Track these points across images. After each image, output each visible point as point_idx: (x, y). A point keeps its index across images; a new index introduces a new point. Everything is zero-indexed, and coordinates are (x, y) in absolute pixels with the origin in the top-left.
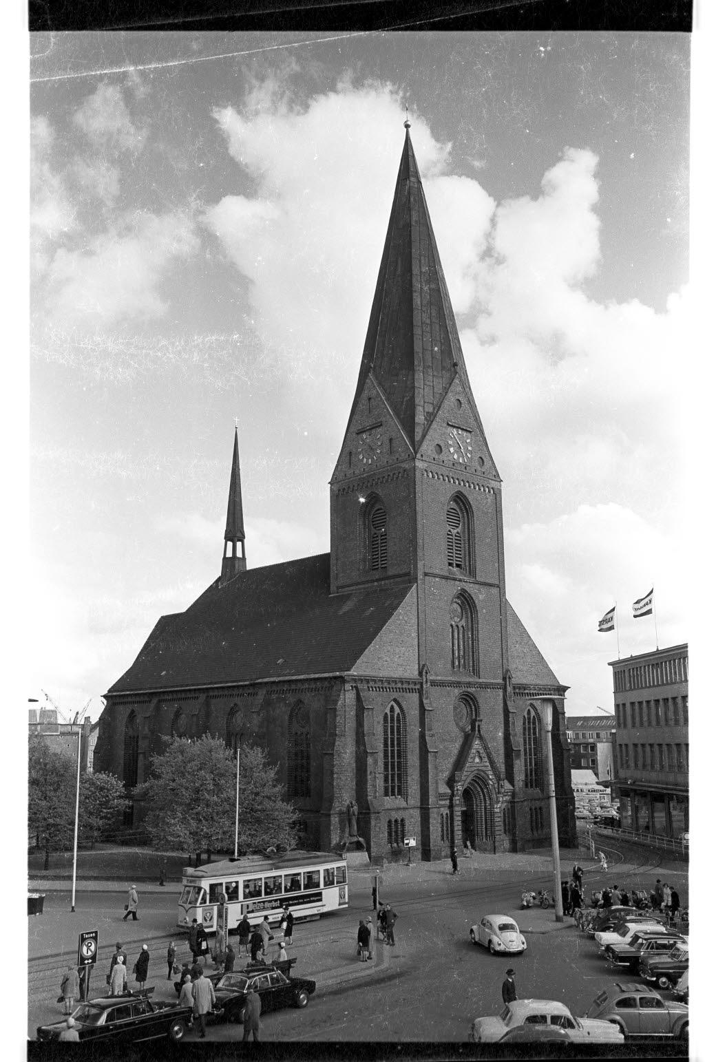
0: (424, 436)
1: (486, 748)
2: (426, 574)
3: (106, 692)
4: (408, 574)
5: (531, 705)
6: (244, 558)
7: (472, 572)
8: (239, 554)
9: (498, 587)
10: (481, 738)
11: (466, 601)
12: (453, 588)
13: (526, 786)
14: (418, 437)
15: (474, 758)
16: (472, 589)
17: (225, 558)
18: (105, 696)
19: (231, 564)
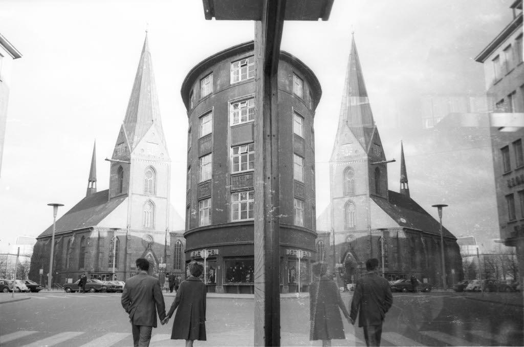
0: (136, 146)
1: (154, 254)
2: (133, 194)
3: (37, 237)
4: (126, 194)
5: (179, 240)
6: (96, 189)
7: (155, 193)
8: (94, 187)
9: (166, 198)
10: (151, 250)
11: (152, 203)
12: (145, 199)
13: (175, 268)
14: (133, 146)
15: (148, 256)
16: (153, 199)
17: (88, 189)
18: (37, 239)
19: (89, 190)
